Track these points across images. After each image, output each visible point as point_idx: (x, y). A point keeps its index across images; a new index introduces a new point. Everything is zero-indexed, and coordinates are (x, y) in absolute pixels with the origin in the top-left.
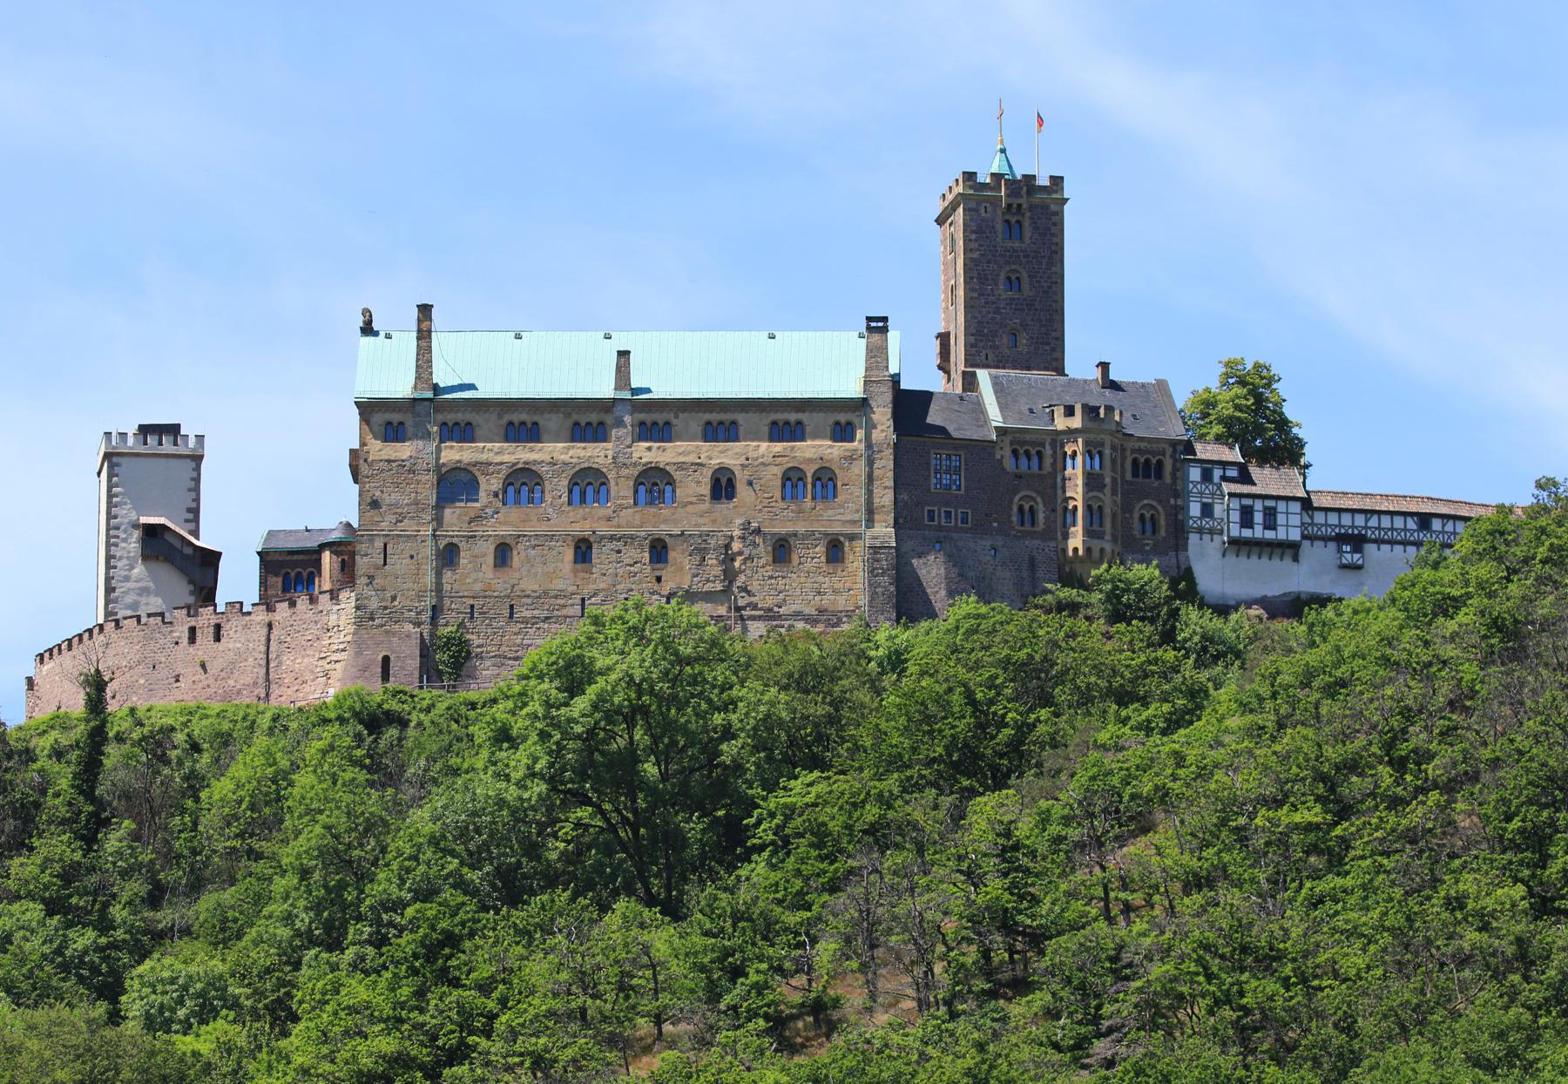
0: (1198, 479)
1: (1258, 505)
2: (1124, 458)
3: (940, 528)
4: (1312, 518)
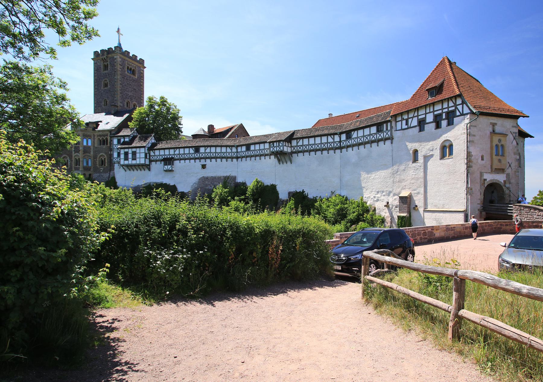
1: (130, 151)
4: (154, 153)
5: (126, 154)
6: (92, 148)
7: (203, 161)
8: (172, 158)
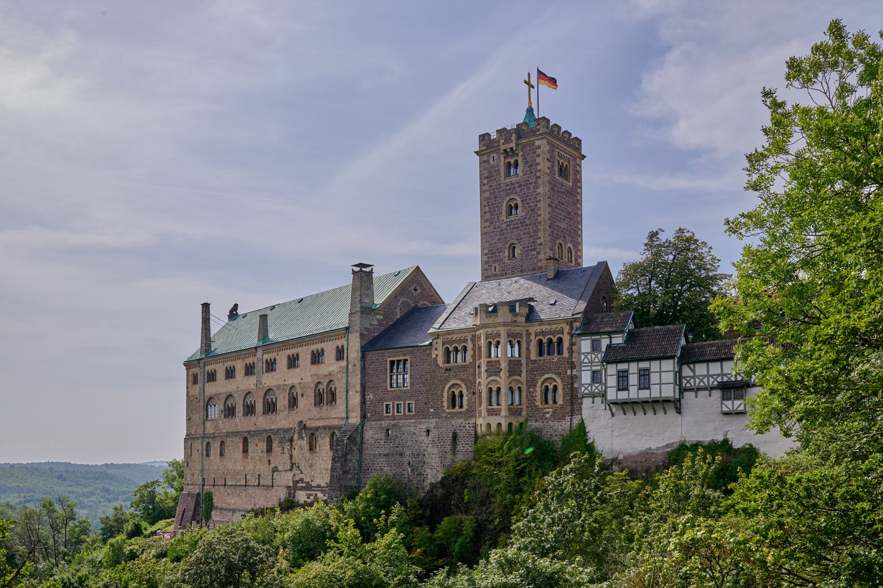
0: (589, 351)
1: (633, 368)
2: (529, 342)
3: (394, 418)
4: (693, 371)
5: (623, 376)
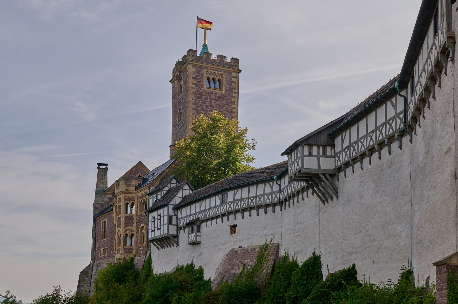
1: (155, 214)
6: (135, 217)
7: (232, 217)
8: (198, 219)
